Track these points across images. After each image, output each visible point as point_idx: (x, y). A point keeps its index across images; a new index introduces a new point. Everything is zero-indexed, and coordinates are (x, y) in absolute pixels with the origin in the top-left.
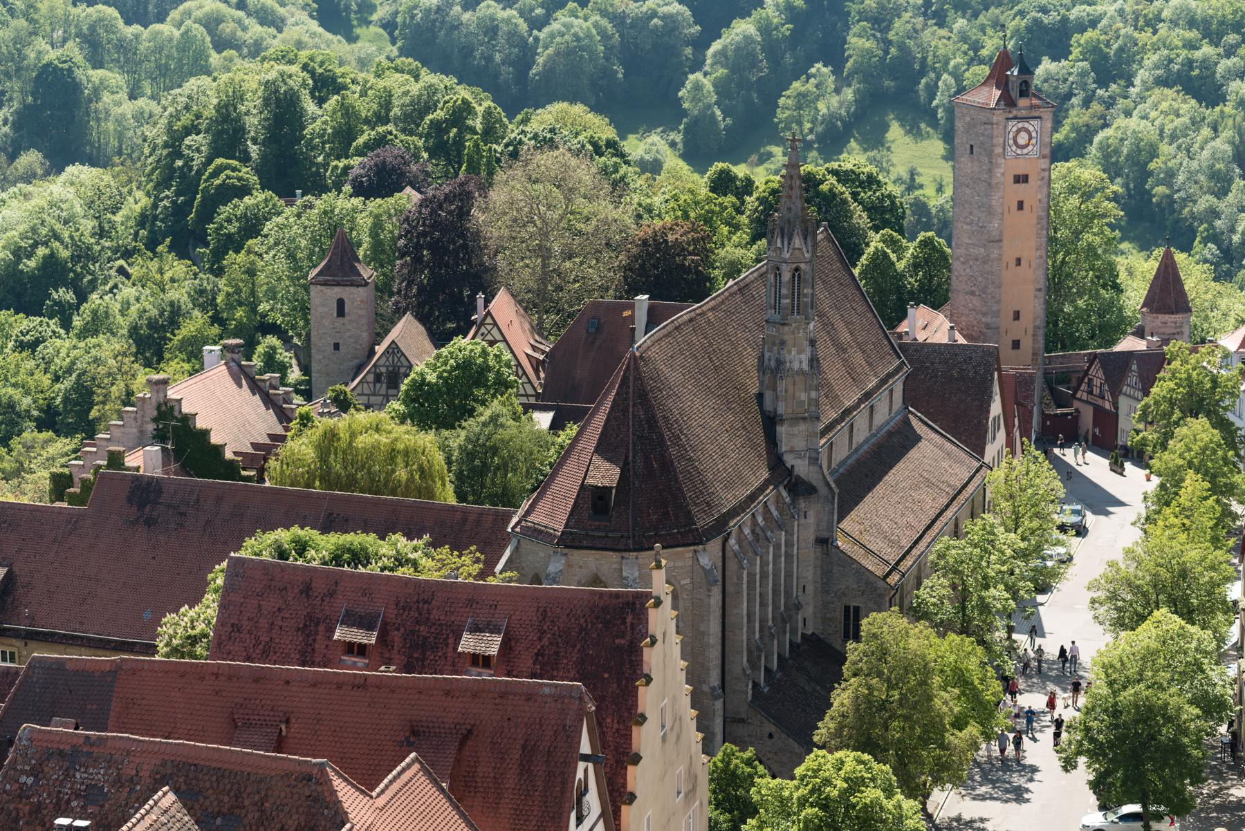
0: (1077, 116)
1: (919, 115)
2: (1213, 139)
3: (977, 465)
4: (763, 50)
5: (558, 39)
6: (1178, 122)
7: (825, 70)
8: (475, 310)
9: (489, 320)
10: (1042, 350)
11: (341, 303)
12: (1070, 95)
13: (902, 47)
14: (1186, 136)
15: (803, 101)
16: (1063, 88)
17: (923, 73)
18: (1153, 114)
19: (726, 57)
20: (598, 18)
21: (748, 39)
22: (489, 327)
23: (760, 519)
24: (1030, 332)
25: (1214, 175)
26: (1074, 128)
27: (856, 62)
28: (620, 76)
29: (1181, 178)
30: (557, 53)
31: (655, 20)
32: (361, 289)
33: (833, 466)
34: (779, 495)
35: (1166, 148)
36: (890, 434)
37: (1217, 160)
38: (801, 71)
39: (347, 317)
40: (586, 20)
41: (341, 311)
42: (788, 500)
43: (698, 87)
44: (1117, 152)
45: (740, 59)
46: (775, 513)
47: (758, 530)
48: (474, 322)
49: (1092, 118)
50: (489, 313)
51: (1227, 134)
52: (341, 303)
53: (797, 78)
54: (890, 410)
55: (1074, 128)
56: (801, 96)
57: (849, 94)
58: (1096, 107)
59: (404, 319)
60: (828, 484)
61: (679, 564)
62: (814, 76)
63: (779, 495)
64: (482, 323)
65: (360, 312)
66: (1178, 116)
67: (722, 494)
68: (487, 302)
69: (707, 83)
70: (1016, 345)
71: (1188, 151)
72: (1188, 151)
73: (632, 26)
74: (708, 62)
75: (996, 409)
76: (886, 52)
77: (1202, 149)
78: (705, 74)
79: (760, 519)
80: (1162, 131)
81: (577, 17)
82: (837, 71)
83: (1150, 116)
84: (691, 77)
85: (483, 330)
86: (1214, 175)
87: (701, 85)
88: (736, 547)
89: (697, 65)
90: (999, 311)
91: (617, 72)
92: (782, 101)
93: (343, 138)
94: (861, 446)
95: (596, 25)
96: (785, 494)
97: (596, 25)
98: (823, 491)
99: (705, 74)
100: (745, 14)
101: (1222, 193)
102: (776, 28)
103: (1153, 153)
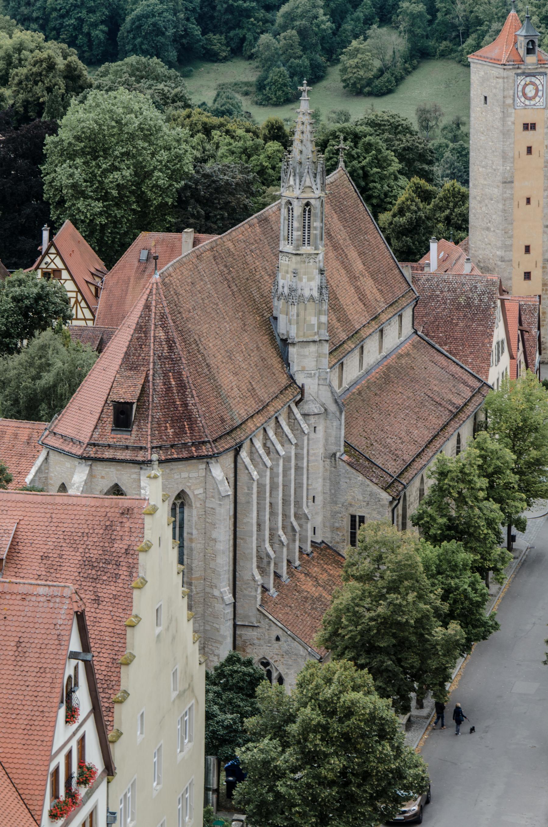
3: (479, 384)
24: (540, 264)
36: (400, 357)
70: (527, 276)
75: (499, 334)
90: (511, 245)
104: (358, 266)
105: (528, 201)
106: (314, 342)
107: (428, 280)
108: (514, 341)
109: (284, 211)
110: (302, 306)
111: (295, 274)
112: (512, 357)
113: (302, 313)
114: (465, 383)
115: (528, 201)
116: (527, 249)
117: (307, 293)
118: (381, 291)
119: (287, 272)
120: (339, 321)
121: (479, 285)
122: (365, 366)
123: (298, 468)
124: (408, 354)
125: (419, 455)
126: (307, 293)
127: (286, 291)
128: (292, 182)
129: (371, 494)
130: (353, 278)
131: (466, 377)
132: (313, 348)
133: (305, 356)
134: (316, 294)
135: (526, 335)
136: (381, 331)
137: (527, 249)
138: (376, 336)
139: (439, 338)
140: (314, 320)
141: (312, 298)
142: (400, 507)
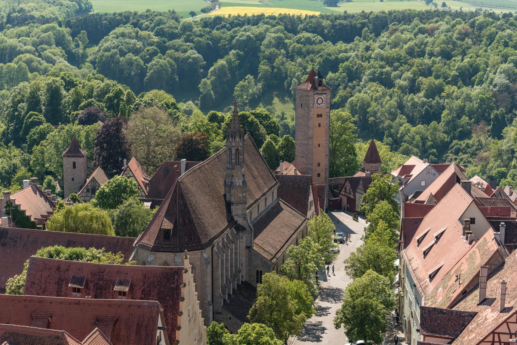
0: (341, 93)
1: (285, 93)
2: (390, 100)
4: (229, 70)
5: (154, 67)
6: (377, 94)
7: (251, 77)
12: (339, 85)
13: (279, 69)
14: (381, 99)
15: (244, 89)
16: (337, 83)
17: (286, 78)
18: (369, 92)
19: (215, 73)
20: (169, 59)
21: (223, 66)
25: (390, 113)
26: (341, 97)
27: (262, 74)
28: (177, 80)
29: (379, 114)
30: (154, 72)
31: (190, 60)
35: (373, 104)
37: (391, 108)
38: (242, 77)
40: (165, 59)
43: (205, 84)
44: (356, 105)
45: (221, 73)
49: (347, 93)
51: (395, 98)
53: (241, 80)
55: (341, 97)
56: (243, 86)
57: (260, 85)
58: (348, 89)
62: (247, 79)
66: (378, 92)
69: (209, 82)
71: (381, 105)
72: (381, 105)
73: (182, 62)
74: (209, 74)
76: (273, 70)
77: (386, 104)
78: (208, 79)
80: (372, 97)
81: (161, 59)
82: (256, 77)
83: (367, 92)
84: (203, 80)
86: (390, 113)
87: (206, 83)
89: (205, 76)
91: (175, 78)
92: (236, 88)
95: (168, 61)
97: (168, 61)
99: (208, 79)
100: (222, 57)
101: (393, 120)
102: (233, 62)
103: (369, 105)
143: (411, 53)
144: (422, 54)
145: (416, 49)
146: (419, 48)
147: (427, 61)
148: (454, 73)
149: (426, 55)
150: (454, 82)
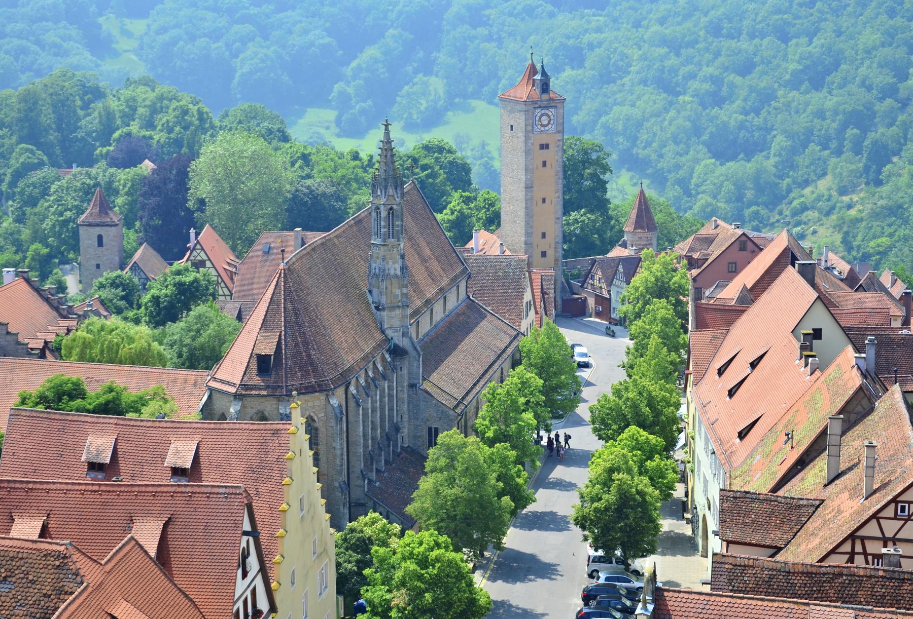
3: (515, 333)
8: (189, 241)
9: (198, 247)
10: (561, 258)
11: (100, 238)
22: (198, 251)
23: (371, 374)
24: (553, 246)
32: (113, 228)
33: (420, 336)
34: (383, 357)
36: (458, 315)
39: (105, 247)
41: (100, 243)
42: (389, 360)
46: (381, 368)
47: (369, 380)
48: (189, 249)
50: (198, 242)
52: (100, 238)
54: (458, 299)
59: (142, 247)
60: (415, 348)
61: (316, 404)
63: (383, 357)
64: (194, 249)
65: (114, 243)
67: (345, 357)
68: (197, 234)
70: (544, 254)
75: (528, 297)
79: (371, 374)
85: (195, 253)
88: (354, 392)
93: (108, 128)
94: (439, 323)
96: (387, 356)
98: (412, 353)
104: (427, 252)
105: (544, 200)
106: (399, 307)
107: (476, 260)
108: (538, 300)
109: (374, 214)
110: (389, 282)
111: (384, 259)
112: (537, 313)
113: (389, 287)
114: (505, 332)
115: (544, 200)
116: (544, 235)
117: (392, 272)
118: (444, 270)
119: (378, 258)
120: (415, 292)
121: (512, 262)
122: (434, 323)
123: (390, 396)
124: (464, 313)
125: (475, 385)
126: (392, 272)
127: (377, 271)
128: (379, 193)
129: (442, 412)
130: (424, 261)
131: (505, 328)
132: (398, 312)
133: (392, 317)
134: (399, 272)
135: (546, 296)
136: (445, 298)
137: (544, 235)
138: (441, 302)
139: (484, 300)
140: (398, 292)
141: (396, 276)
142: (463, 420)
143: (716, 30)
144: (734, 35)
145: (726, 25)
146: (730, 21)
147: (745, 45)
148: (793, 66)
149: (744, 36)
150: (795, 83)
